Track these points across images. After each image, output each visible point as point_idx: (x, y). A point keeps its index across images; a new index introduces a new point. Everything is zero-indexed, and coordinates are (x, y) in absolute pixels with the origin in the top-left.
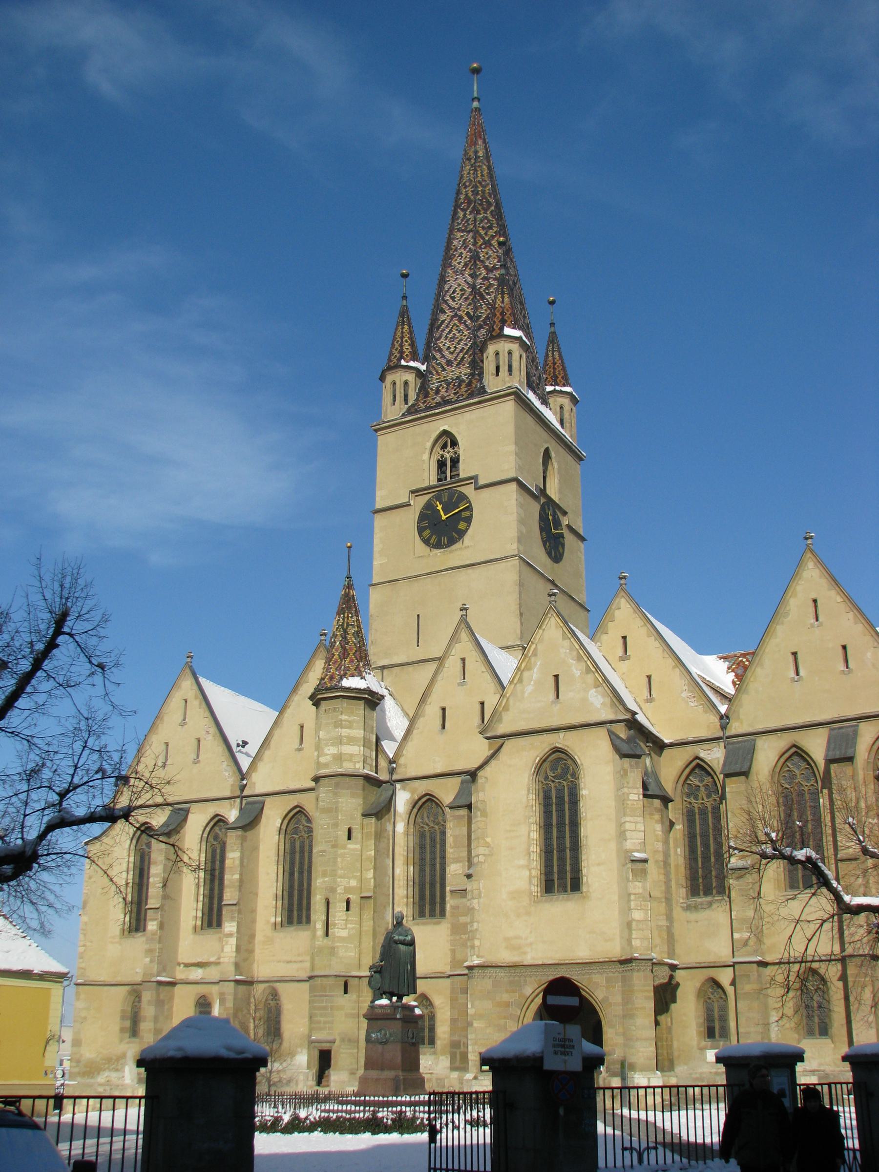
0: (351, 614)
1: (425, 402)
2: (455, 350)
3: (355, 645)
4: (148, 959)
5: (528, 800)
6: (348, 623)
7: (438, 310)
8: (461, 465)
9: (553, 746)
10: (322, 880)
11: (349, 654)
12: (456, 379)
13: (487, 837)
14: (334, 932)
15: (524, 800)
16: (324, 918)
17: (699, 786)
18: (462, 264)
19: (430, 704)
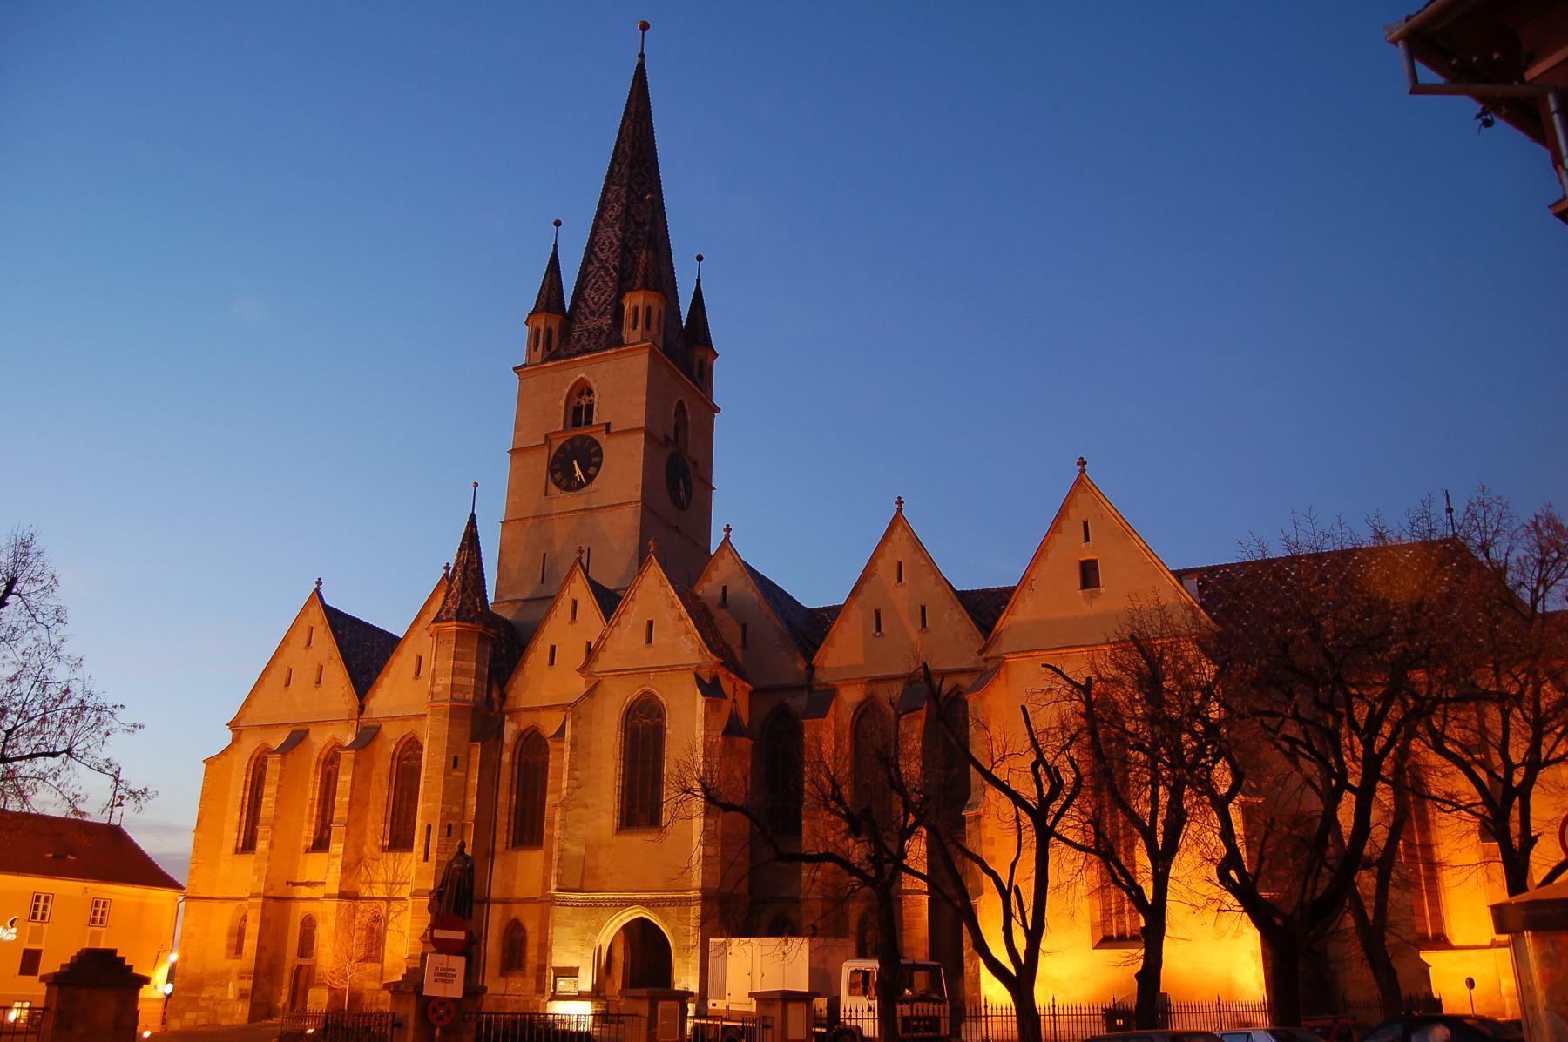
4: (256, 878)
11: (466, 590)
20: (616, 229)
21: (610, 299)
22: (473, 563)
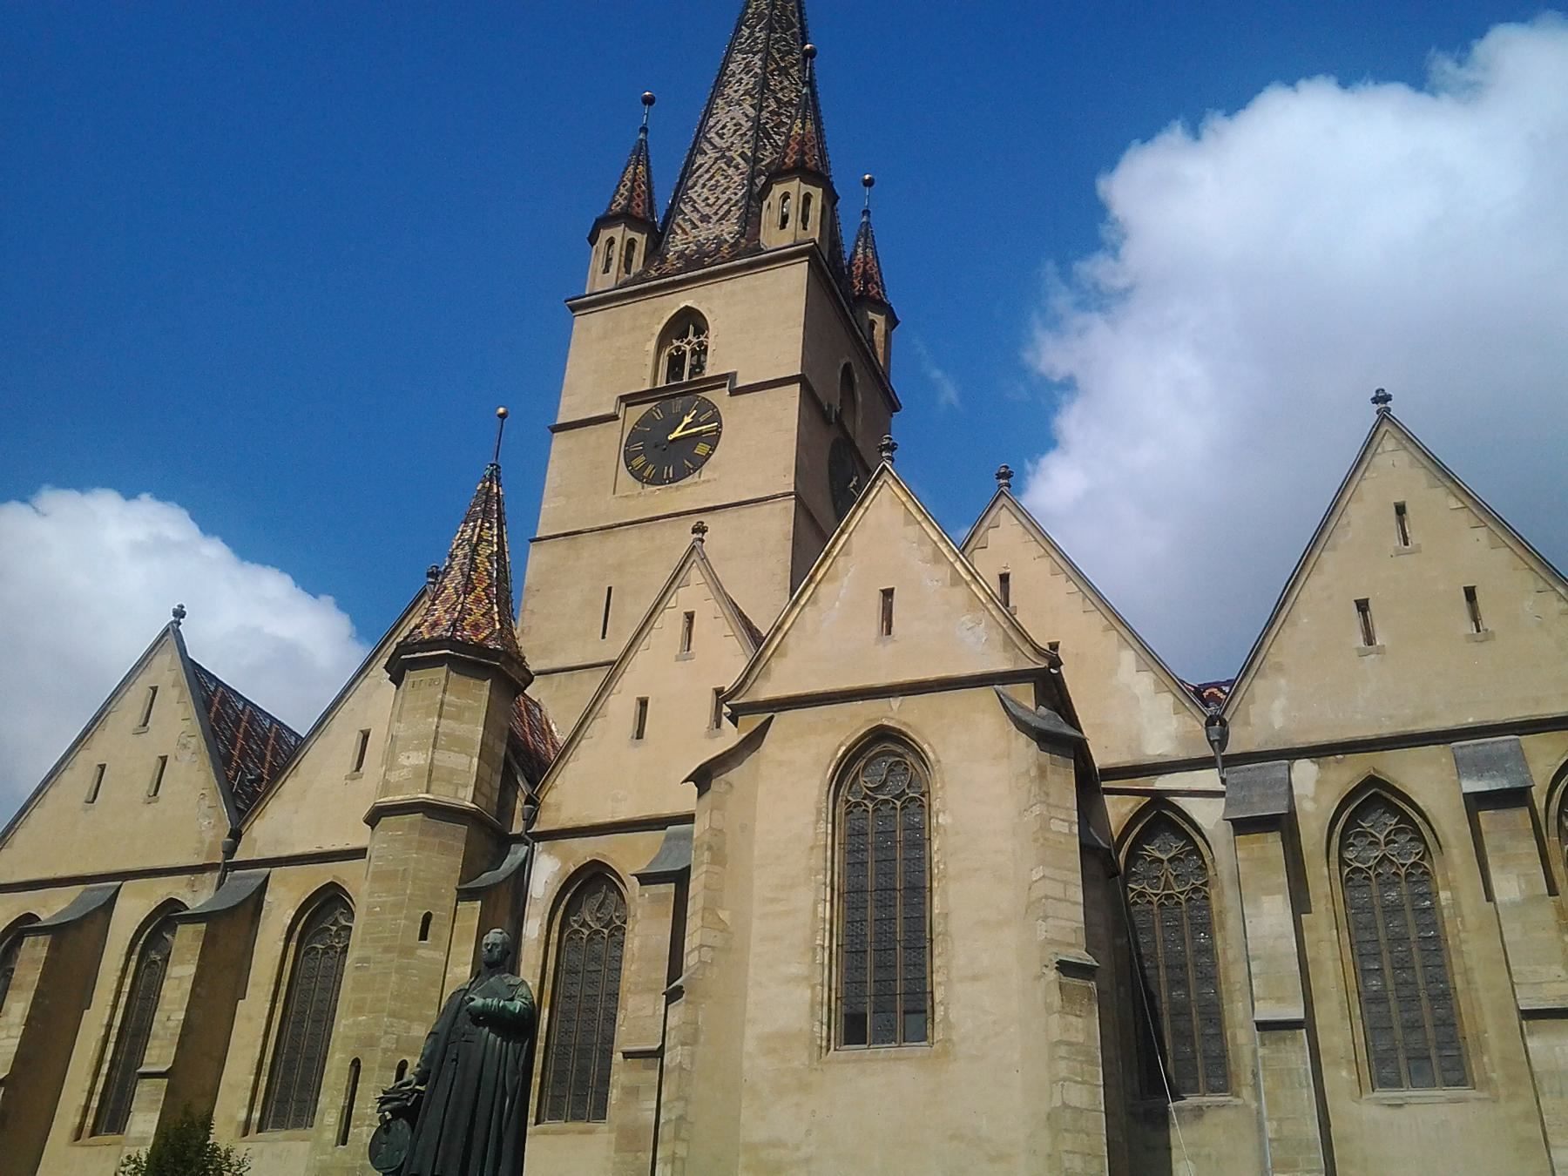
0: (491, 523)
1: (660, 268)
2: (716, 201)
3: (490, 575)
5: (816, 834)
6: (480, 536)
7: (696, 150)
8: (710, 359)
11: (474, 588)
12: (714, 239)
13: (721, 908)
15: (811, 832)
16: (341, 1101)
17: (1162, 861)
19: (620, 692)
20: (746, 106)
21: (735, 198)
22: (491, 543)
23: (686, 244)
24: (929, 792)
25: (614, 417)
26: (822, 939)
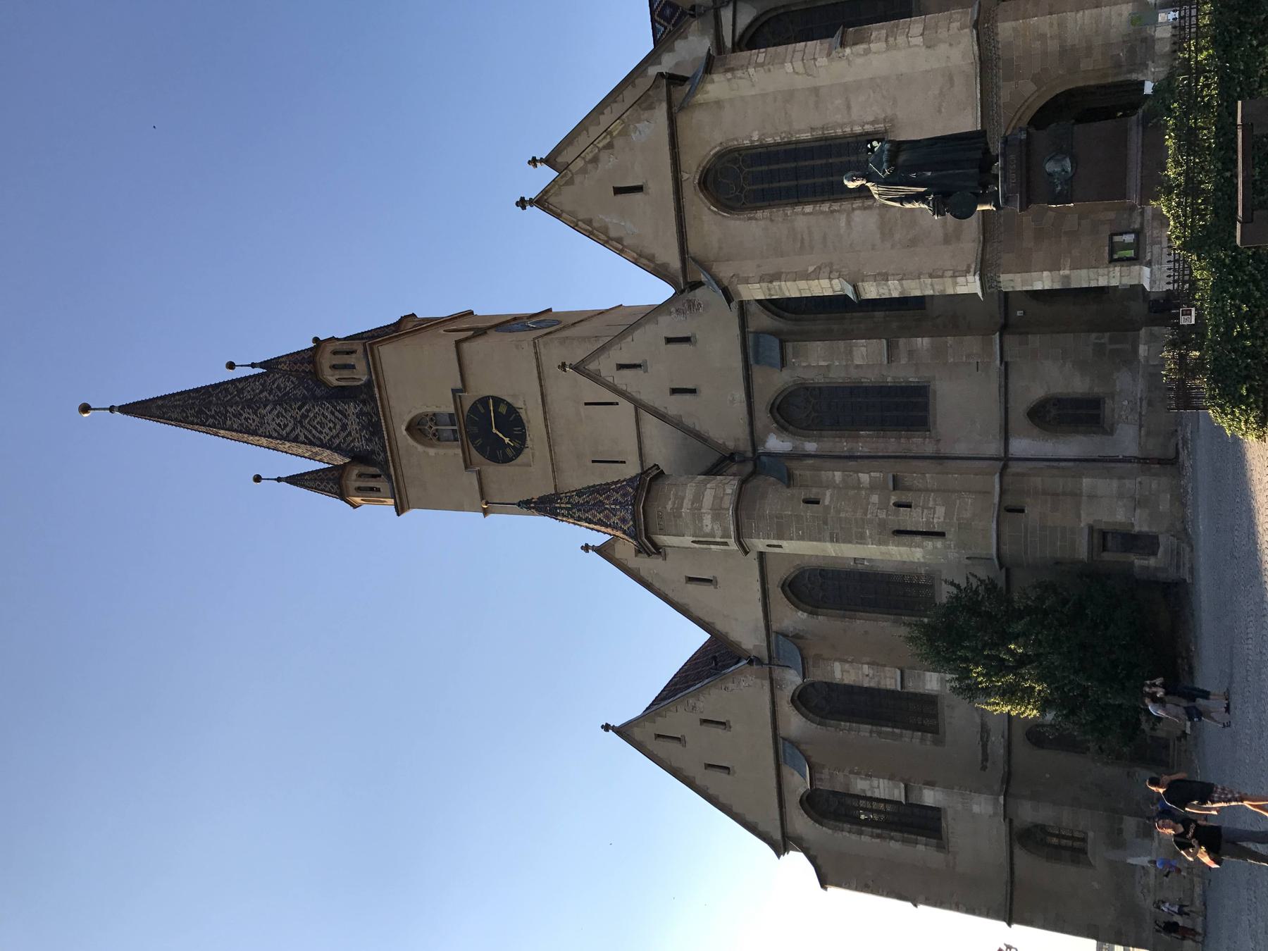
0: (557, 500)
2: (332, 421)
5: (763, 218)
6: (567, 503)
9: (698, 188)
10: (869, 540)
11: (600, 501)
12: (359, 418)
14: (938, 523)
15: (762, 223)
18: (255, 417)
19: (666, 408)
20: (264, 412)
23: (361, 438)
24: (739, 151)
25: (479, 473)
26: (825, 207)
